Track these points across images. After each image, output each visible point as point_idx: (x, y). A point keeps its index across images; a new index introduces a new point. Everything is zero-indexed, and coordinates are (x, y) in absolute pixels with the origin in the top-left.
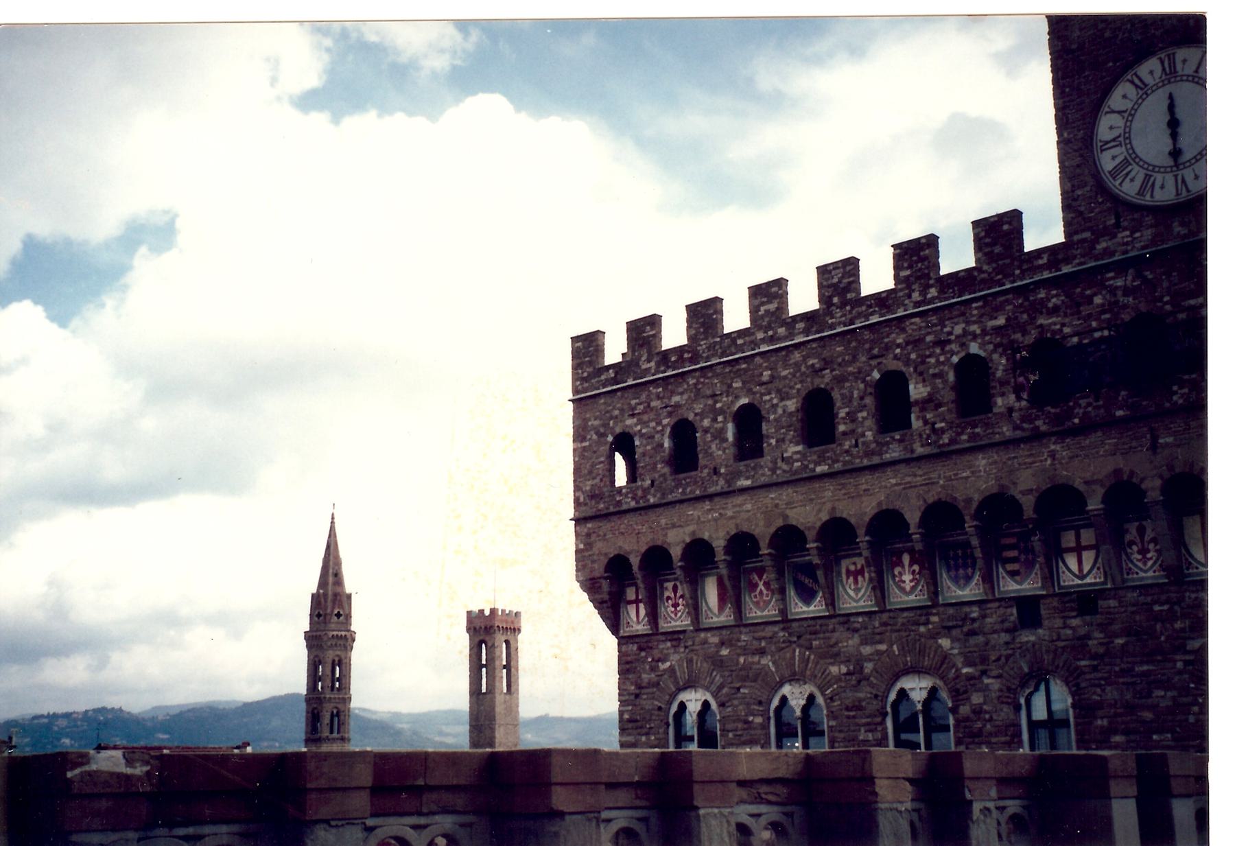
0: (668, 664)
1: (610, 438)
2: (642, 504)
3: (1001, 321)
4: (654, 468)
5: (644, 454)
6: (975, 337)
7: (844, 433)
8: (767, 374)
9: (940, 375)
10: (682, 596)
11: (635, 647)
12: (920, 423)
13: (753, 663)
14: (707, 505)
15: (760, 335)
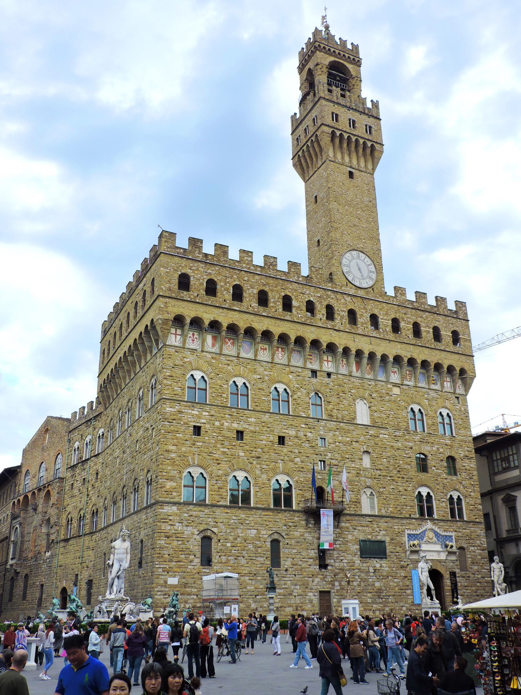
0: (189, 360)
1: (180, 273)
2: (193, 300)
3: (319, 295)
4: (199, 291)
5: (195, 284)
6: (312, 296)
7: (272, 306)
8: (246, 279)
9: (302, 302)
10: (197, 338)
11: (174, 350)
12: (296, 313)
13: (224, 367)
14: (221, 310)
15: (244, 265)
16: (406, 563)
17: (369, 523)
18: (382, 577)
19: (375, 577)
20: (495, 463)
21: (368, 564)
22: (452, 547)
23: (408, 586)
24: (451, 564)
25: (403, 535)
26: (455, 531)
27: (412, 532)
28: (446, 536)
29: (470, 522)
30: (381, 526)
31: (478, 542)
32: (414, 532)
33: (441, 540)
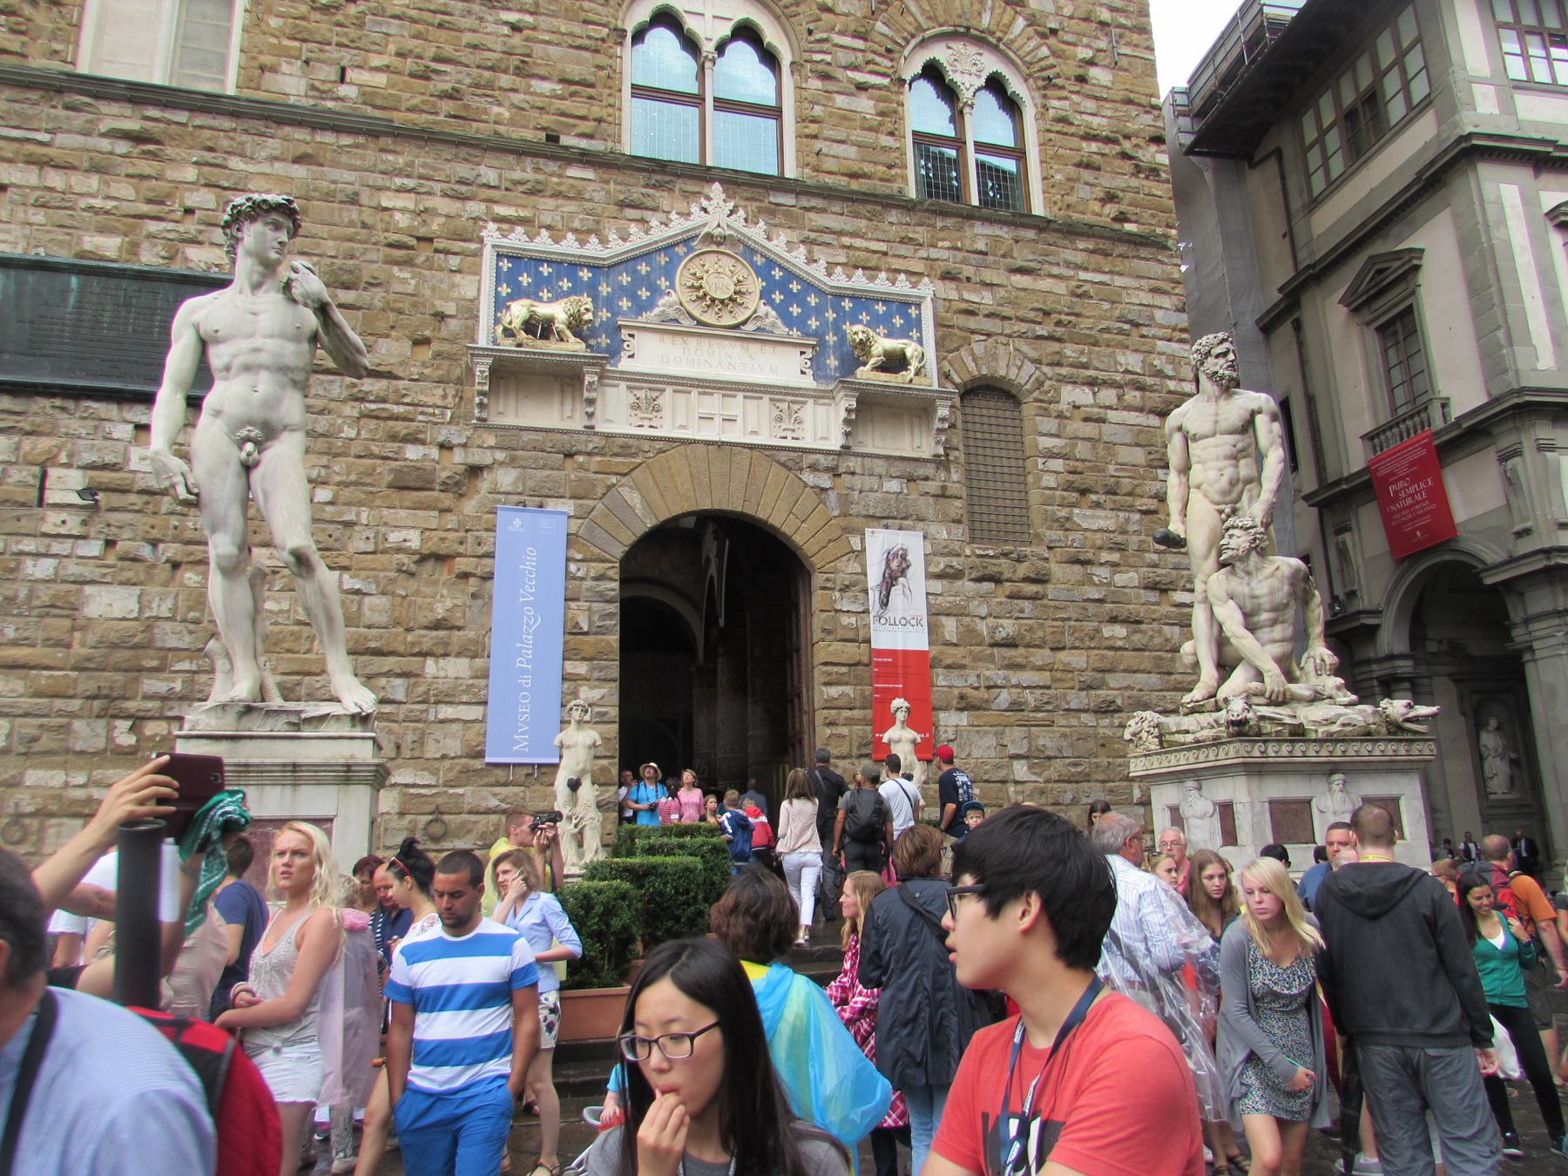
16: (458, 457)
17: (123, 147)
18: (171, 550)
19: (94, 548)
20: (1314, 158)
21: (45, 443)
22: (895, 362)
23: (437, 625)
24: (893, 486)
25: (454, 262)
26: (947, 276)
27: (543, 243)
28: (862, 300)
29: (1071, 231)
30: (248, 176)
31: (1132, 361)
32: (569, 246)
33: (813, 323)
